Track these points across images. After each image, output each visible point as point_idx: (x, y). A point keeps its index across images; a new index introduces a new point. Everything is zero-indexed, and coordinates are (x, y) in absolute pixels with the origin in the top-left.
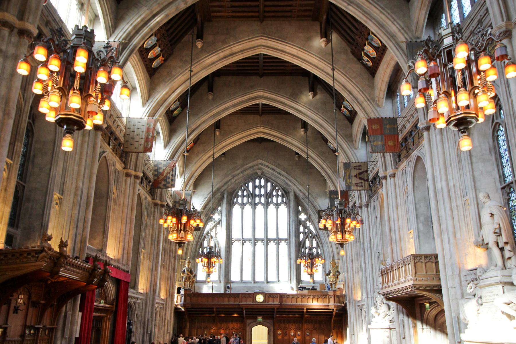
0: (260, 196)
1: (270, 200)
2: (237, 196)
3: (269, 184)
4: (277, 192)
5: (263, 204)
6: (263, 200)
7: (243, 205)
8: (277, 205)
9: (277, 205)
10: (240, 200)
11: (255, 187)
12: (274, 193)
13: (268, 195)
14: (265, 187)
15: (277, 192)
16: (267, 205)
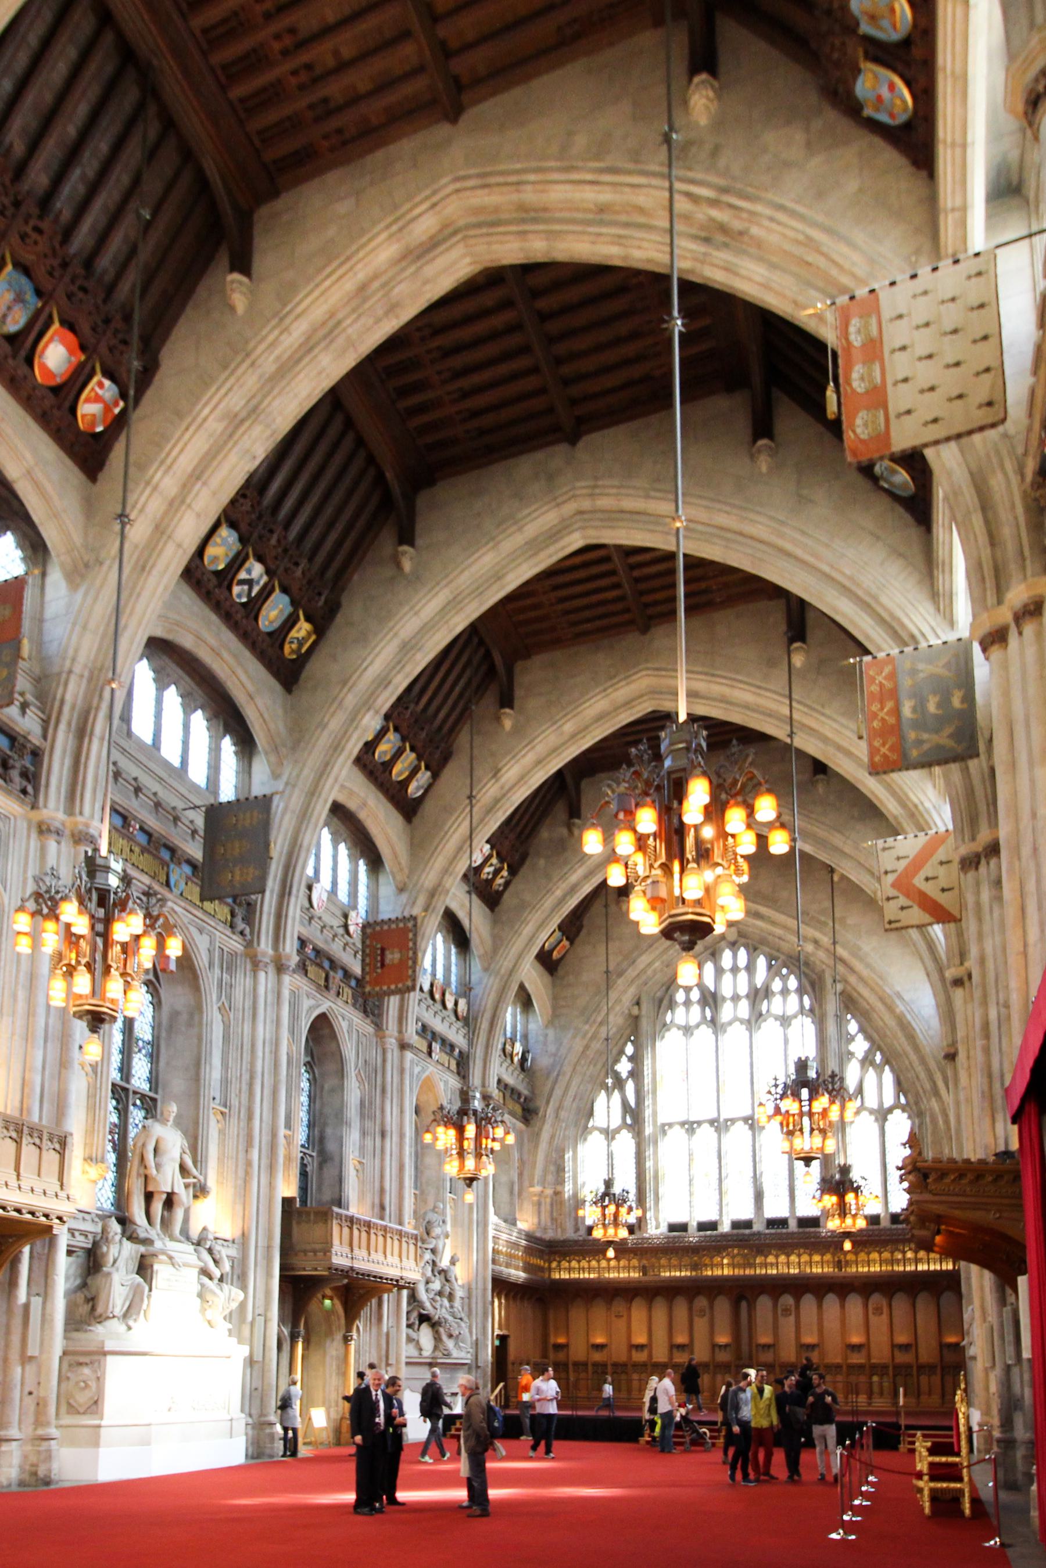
0: (736, 998)
1: (764, 1007)
2: (672, 1005)
3: (761, 962)
4: (784, 979)
5: (742, 1021)
6: (744, 1009)
7: (687, 1030)
8: (785, 1021)
9: (785, 1021)
10: (679, 1015)
11: (719, 971)
12: (777, 985)
13: (758, 995)
14: (750, 968)
15: (784, 979)
16: (756, 1018)
